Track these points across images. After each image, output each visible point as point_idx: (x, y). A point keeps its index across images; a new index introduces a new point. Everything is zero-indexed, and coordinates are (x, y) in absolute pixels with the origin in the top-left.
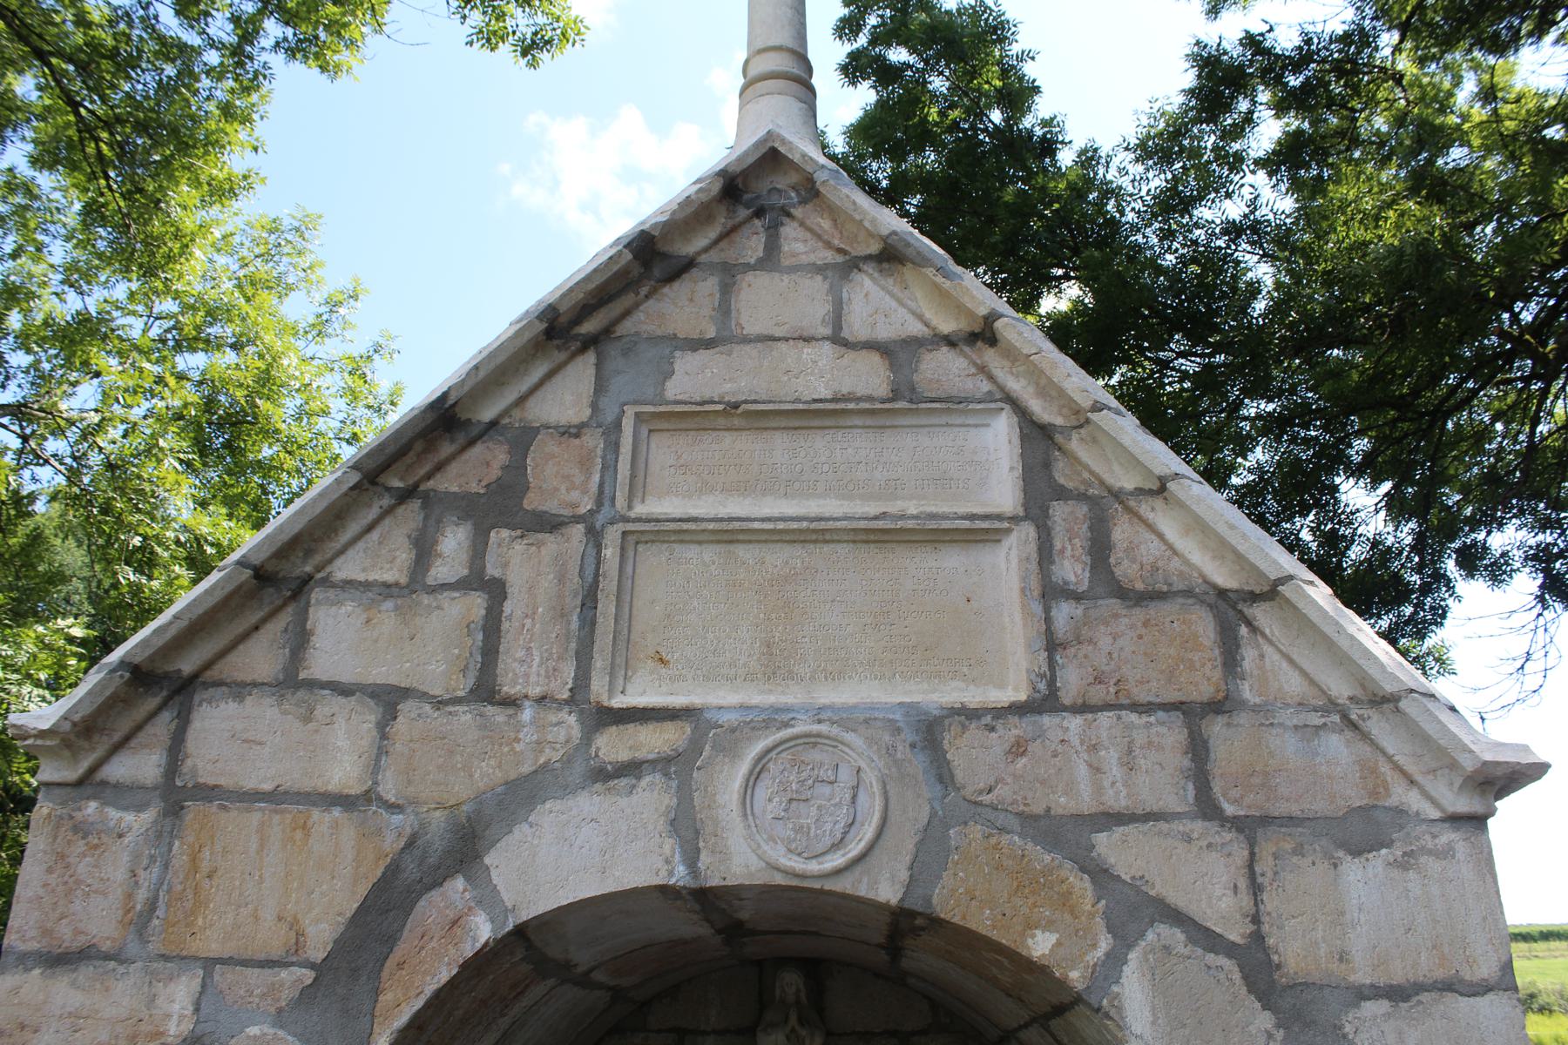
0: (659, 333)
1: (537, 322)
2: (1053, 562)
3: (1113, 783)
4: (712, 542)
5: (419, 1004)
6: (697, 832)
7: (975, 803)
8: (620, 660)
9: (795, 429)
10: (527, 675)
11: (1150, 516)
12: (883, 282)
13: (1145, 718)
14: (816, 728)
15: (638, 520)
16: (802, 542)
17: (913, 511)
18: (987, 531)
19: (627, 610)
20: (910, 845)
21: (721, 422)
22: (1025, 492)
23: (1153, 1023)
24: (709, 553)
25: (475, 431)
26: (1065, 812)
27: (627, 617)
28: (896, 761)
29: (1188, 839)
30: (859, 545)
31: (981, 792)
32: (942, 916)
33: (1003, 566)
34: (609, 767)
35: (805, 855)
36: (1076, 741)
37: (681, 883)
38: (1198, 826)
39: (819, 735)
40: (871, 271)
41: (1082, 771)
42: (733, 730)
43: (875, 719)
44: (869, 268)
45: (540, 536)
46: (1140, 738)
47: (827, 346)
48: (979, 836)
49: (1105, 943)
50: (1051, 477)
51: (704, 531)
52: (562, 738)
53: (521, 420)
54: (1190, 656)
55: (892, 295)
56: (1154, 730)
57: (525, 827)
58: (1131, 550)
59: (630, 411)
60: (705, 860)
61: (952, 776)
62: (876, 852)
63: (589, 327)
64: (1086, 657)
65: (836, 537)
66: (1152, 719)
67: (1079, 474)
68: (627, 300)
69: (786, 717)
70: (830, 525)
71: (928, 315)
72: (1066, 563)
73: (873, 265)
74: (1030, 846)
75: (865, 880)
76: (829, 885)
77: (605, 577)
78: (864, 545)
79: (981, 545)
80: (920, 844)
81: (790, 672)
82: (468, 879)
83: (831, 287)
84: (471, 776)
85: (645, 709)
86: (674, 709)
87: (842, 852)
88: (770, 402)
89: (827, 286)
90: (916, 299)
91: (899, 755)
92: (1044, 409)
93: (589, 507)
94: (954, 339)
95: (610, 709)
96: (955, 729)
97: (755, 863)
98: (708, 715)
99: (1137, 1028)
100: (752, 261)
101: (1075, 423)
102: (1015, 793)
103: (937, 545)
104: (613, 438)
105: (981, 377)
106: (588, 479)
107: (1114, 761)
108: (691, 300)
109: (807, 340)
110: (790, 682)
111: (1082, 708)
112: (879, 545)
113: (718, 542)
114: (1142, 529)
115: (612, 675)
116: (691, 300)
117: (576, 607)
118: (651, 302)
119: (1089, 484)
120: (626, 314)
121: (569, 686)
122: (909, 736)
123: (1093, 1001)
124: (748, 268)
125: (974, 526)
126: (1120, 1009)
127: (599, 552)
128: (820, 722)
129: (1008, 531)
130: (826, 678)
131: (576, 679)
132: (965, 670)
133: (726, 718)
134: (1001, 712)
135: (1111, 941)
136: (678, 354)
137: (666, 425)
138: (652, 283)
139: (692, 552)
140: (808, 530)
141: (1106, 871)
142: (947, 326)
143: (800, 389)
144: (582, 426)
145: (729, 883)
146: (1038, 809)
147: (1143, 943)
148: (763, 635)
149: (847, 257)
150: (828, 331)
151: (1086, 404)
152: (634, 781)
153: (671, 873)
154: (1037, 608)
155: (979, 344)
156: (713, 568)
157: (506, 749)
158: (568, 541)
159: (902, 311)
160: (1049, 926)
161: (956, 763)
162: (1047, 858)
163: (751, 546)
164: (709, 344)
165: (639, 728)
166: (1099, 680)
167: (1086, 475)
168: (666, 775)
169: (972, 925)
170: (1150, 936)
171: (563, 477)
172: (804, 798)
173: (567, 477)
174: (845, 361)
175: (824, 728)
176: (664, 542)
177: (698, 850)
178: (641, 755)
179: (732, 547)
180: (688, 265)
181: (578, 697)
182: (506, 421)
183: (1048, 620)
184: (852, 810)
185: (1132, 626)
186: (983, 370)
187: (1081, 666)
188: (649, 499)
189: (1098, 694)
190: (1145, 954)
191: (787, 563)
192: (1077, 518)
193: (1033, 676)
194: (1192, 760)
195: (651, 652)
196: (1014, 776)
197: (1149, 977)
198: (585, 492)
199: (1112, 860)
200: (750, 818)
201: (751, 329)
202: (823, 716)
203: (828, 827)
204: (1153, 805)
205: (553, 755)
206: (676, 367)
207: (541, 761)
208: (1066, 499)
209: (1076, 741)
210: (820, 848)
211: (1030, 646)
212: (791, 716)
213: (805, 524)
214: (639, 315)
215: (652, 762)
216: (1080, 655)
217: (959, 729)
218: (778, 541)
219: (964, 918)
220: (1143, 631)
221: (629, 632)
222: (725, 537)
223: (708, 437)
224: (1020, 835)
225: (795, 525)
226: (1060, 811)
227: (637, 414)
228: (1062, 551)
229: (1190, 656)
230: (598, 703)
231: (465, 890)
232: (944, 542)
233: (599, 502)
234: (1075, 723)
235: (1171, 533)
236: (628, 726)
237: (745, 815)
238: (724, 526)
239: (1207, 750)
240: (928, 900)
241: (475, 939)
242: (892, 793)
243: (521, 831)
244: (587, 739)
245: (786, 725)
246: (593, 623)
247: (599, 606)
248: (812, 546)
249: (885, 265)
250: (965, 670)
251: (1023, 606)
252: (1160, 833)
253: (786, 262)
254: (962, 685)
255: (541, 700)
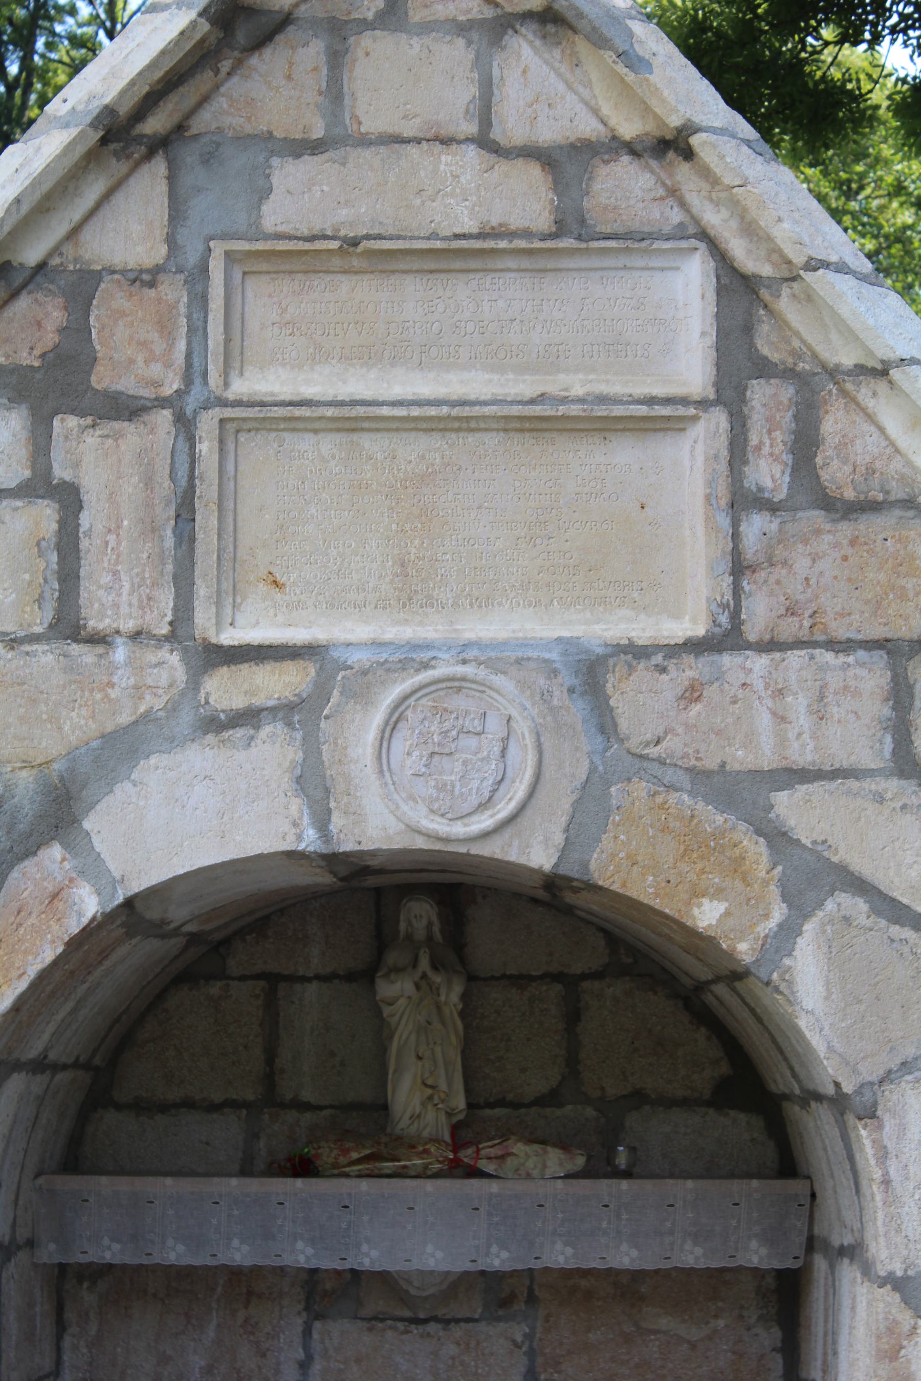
0: (249, 129)
1: (91, 132)
2: (746, 462)
3: (800, 735)
4: (330, 430)
5: (22, 985)
6: (327, 791)
7: (641, 756)
8: (226, 585)
9: (431, 272)
10: (116, 606)
11: (870, 403)
12: (546, 56)
13: (842, 658)
14: (461, 670)
15: (238, 403)
16: (441, 430)
17: (578, 391)
18: (668, 418)
19: (230, 520)
20: (566, 804)
21: (336, 262)
22: (718, 366)
23: (826, 998)
24: (328, 444)
25: (18, 281)
26: (742, 768)
27: (231, 528)
28: (551, 709)
29: (880, 799)
30: (511, 434)
31: (647, 744)
32: (600, 883)
33: (687, 463)
34: (222, 716)
35: (449, 816)
36: (759, 685)
37: (311, 849)
38: (893, 785)
39: (463, 679)
40: (530, 36)
41: (765, 720)
42: (365, 673)
43: (529, 659)
44: (528, 30)
45: (117, 425)
46: (834, 681)
47: (471, 152)
48: (644, 794)
49: (778, 913)
50: (752, 346)
51: (320, 418)
52: (164, 681)
53: (76, 260)
54: (903, 582)
55: (559, 75)
56: (851, 673)
57: (127, 785)
58: (843, 445)
59: (218, 249)
60: (337, 822)
61: (615, 725)
62: (529, 812)
63: (155, 125)
64: (778, 582)
65: (482, 425)
66: (851, 659)
67: (788, 342)
68: (204, 80)
69: (425, 656)
70: (477, 411)
71: (606, 110)
72: (762, 463)
73: (535, 26)
74: (701, 805)
75: (516, 843)
76: (477, 849)
77: (202, 479)
78: (518, 435)
79: (661, 434)
80: (577, 804)
81: (429, 597)
82: (66, 846)
83: (477, 57)
84: (60, 728)
85: (260, 647)
86: (295, 646)
87: (489, 812)
88: (399, 237)
89: (472, 56)
90: (589, 85)
91: (555, 702)
92: (749, 252)
93: (175, 387)
94: (639, 148)
95: (219, 648)
96: (621, 669)
97: (394, 827)
98: (335, 654)
99: (808, 1002)
100: (370, 15)
101: (787, 275)
102: (686, 745)
103: (607, 435)
104: (199, 288)
105: (670, 201)
106: (171, 346)
107: (802, 709)
108: (289, 78)
109: (447, 141)
110: (429, 610)
111: (770, 646)
112: (535, 434)
113: (338, 430)
114: (859, 418)
115: (219, 604)
116: (289, 78)
117: (168, 519)
118: (235, 79)
119: (797, 355)
120: (205, 99)
121: (169, 618)
122: (567, 679)
123: (763, 974)
124: (365, 25)
125: (653, 413)
126: (790, 983)
127: (192, 447)
128: (464, 662)
129: (695, 419)
130: (471, 605)
131: (176, 609)
132: (635, 595)
133: (357, 658)
134: (675, 650)
135: (786, 911)
136: (275, 161)
137: (265, 267)
138: (236, 54)
139: (305, 443)
140: (449, 417)
141: (784, 834)
142: (629, 129)
143: (437, 218)
144: (157, 270)
145: (365, 847)
146: (711, 763)
147: (820, 914)
148: (396, 552)
149: (499, 11)
150: (472, 128)
151: (799, 259)
152: (252, 732)
153: (299, 838)
154: (724, 521)
155: (671, 155)
156: (333, 463)
157: (99, 696)
158: (152, 431)
159: (570, 98)
160: (718, 894)
161: (620, 711)
162: (720, 819)
163: (379, 435)
164: (315, 147)
165: (254, 668)
166: (791, 611)
167: (796, 343)
168: (289, 724)
169: (633, 892)
170: (830, 905)
171: (139, 343)
172: (447, 751)
173: (144, 344)
174: (495, 175)
175: (468, 670)
176: (270, 430)
177: (329, 812)
178: (258, 701)
179: (355, 437)
180: (285, 21)
181: (180, 632)
182: (55, 261)
183: (736, 536)
184: (501, 766)
185: (836, 545)
186: (674, 193)
187: (771, 594)
188: (249, 371)
189: (789, 629)
190: (823, 924)
191: (423, 457)
192: (781, 403)
193: (714, 607)
194: (893, 709)
195: (263, 573)
196: (686, 725)
197: (825, 949)
198: (168, 365)
199: (792, 822)
200: (387, 774)
201: (372, 125)
202: (471, 654)
203: (475, 784)
204: (843, 760)
205: (154, 702)
206: (275, 181)
207: (142, 709)
208: (769, 377)
209: (759, 685)
210: (466, 808)
211: (712, 569)
212: (431, 654)
213: (445, 410)
214: (220, 102)
215: (273, 710)
216: (772, 579)
217: (625, 669)
218: (411, 430)
219: (624, 885)
220: (849, 551)
221: (235, 547)
222: (347, 425)
223: (319, 281)
224: (690, 793)
225: (432, 411)
226: (737, 767)
227: (228, 254)
228: (758, 448)
229: (903, 582)
230: (204, 639)
231: (64, 860)
232: (616, 430)
233: (188, 380)
234: (759, 663)
235: (893, 428)
236: (241, 667)
237: (381, 772)
238: (345, 412)
239: (912, 696)
240: (585, 865)
241: (80, 914)
242: (547, 746)
243: (123, 791)
244: (194, 683)
245: (426, 666)
246: (192, 540)
247: (198, 518)
248: (454, 435)
249: (551, 28)
250: (635, 595)
251: (708, 519)
252: (848, 792)
253: (416, 16)
254: (629, 613)
255: (136, 636)
